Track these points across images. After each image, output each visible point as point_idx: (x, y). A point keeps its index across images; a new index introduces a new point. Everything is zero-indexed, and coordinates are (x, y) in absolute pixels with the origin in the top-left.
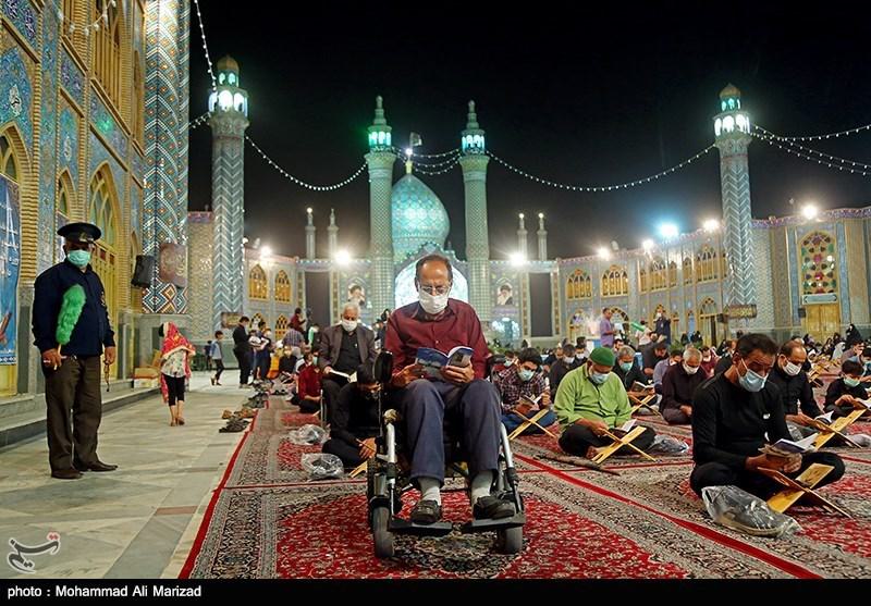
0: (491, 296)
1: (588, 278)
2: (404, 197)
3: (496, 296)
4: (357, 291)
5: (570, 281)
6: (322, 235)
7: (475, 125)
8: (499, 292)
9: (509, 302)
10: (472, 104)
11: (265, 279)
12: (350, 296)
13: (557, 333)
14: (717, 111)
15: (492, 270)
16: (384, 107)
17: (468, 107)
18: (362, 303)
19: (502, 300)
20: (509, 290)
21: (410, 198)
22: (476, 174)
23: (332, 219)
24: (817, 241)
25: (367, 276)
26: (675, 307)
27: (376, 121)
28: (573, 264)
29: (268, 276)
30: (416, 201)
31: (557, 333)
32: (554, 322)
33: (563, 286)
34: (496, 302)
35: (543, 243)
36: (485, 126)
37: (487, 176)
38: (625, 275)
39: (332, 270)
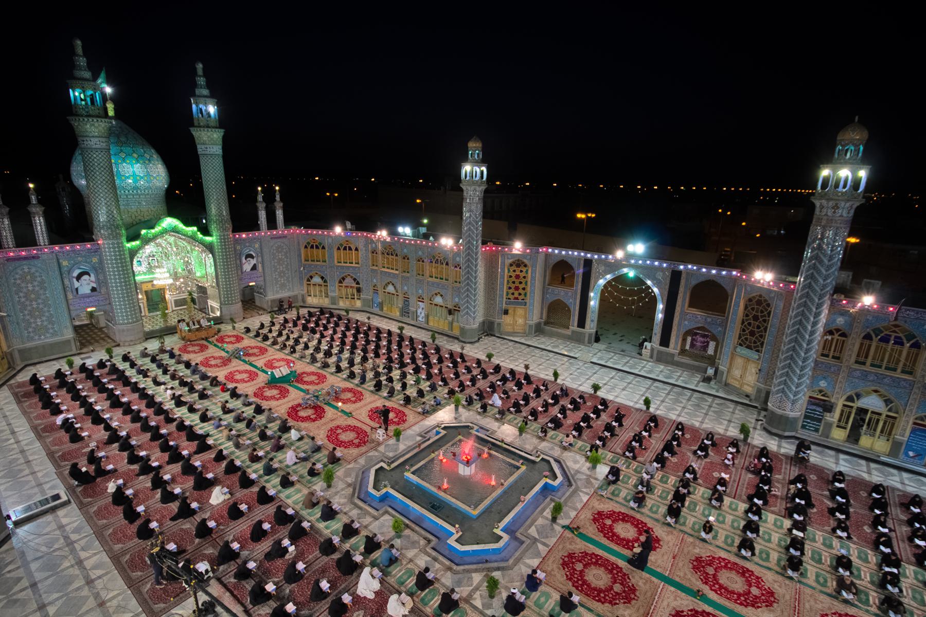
1: (323, 248)
5: (306, 247)
7: (205, 92)
10: (200, 66)
14: (465, 159)
17: (195, 69)
21: (121, 151)
22: (210, 144)
24: (518, 266)
26: (406, 288)
28: (308, 234)
30: (128, 155)
35: (280, 214)
36: (216, 95)
37: (224, 148)
38: (356, 249)
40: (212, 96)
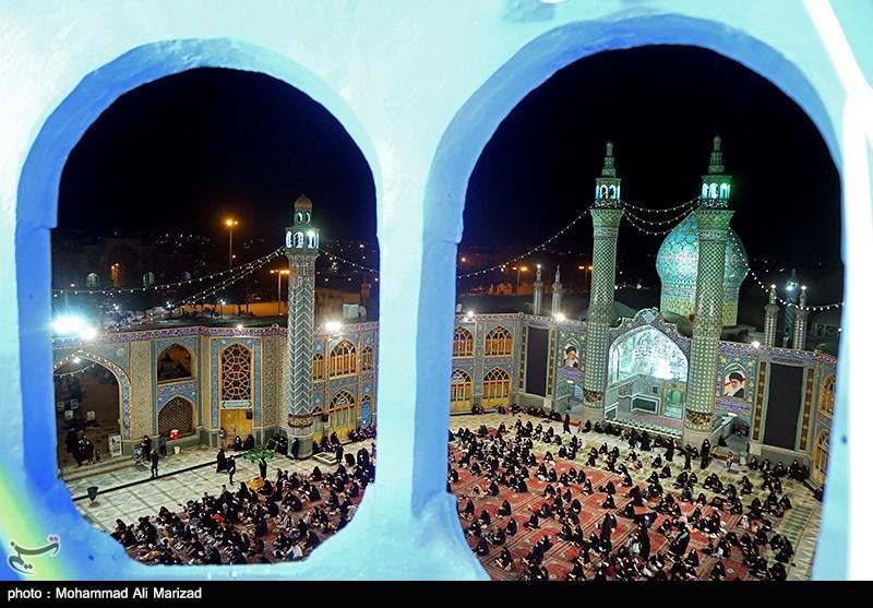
0: (716, 384)
2: (680, 237)
3: (723, 384)
4: (573, 352)
6: (547, 298)
8: (727, 381)
9: (740, 394)
11: (471, 337)
12: (566, 357)
13: (803, 447)
15: (722, 352)
16: (614, 154)
18: (576, 365)
19: (731, 390)
20: (741, 380)
23: (557, 277)
25: (583, 338)
27: (605, 172)
29: (475, 339)
31: (803, 447)
32: (799, 432)
33: (818, 388)
34: (722, 390)
39: (551, 328)
40: (725, 173)
